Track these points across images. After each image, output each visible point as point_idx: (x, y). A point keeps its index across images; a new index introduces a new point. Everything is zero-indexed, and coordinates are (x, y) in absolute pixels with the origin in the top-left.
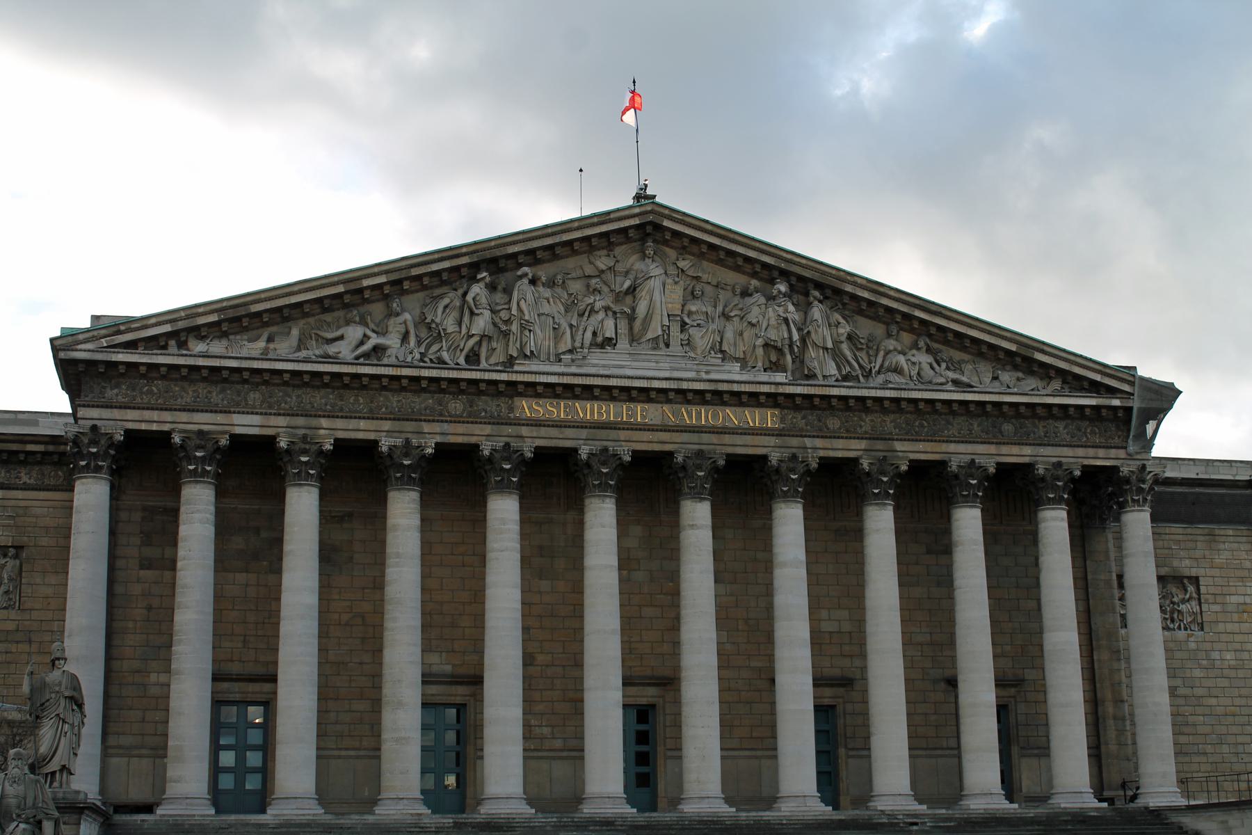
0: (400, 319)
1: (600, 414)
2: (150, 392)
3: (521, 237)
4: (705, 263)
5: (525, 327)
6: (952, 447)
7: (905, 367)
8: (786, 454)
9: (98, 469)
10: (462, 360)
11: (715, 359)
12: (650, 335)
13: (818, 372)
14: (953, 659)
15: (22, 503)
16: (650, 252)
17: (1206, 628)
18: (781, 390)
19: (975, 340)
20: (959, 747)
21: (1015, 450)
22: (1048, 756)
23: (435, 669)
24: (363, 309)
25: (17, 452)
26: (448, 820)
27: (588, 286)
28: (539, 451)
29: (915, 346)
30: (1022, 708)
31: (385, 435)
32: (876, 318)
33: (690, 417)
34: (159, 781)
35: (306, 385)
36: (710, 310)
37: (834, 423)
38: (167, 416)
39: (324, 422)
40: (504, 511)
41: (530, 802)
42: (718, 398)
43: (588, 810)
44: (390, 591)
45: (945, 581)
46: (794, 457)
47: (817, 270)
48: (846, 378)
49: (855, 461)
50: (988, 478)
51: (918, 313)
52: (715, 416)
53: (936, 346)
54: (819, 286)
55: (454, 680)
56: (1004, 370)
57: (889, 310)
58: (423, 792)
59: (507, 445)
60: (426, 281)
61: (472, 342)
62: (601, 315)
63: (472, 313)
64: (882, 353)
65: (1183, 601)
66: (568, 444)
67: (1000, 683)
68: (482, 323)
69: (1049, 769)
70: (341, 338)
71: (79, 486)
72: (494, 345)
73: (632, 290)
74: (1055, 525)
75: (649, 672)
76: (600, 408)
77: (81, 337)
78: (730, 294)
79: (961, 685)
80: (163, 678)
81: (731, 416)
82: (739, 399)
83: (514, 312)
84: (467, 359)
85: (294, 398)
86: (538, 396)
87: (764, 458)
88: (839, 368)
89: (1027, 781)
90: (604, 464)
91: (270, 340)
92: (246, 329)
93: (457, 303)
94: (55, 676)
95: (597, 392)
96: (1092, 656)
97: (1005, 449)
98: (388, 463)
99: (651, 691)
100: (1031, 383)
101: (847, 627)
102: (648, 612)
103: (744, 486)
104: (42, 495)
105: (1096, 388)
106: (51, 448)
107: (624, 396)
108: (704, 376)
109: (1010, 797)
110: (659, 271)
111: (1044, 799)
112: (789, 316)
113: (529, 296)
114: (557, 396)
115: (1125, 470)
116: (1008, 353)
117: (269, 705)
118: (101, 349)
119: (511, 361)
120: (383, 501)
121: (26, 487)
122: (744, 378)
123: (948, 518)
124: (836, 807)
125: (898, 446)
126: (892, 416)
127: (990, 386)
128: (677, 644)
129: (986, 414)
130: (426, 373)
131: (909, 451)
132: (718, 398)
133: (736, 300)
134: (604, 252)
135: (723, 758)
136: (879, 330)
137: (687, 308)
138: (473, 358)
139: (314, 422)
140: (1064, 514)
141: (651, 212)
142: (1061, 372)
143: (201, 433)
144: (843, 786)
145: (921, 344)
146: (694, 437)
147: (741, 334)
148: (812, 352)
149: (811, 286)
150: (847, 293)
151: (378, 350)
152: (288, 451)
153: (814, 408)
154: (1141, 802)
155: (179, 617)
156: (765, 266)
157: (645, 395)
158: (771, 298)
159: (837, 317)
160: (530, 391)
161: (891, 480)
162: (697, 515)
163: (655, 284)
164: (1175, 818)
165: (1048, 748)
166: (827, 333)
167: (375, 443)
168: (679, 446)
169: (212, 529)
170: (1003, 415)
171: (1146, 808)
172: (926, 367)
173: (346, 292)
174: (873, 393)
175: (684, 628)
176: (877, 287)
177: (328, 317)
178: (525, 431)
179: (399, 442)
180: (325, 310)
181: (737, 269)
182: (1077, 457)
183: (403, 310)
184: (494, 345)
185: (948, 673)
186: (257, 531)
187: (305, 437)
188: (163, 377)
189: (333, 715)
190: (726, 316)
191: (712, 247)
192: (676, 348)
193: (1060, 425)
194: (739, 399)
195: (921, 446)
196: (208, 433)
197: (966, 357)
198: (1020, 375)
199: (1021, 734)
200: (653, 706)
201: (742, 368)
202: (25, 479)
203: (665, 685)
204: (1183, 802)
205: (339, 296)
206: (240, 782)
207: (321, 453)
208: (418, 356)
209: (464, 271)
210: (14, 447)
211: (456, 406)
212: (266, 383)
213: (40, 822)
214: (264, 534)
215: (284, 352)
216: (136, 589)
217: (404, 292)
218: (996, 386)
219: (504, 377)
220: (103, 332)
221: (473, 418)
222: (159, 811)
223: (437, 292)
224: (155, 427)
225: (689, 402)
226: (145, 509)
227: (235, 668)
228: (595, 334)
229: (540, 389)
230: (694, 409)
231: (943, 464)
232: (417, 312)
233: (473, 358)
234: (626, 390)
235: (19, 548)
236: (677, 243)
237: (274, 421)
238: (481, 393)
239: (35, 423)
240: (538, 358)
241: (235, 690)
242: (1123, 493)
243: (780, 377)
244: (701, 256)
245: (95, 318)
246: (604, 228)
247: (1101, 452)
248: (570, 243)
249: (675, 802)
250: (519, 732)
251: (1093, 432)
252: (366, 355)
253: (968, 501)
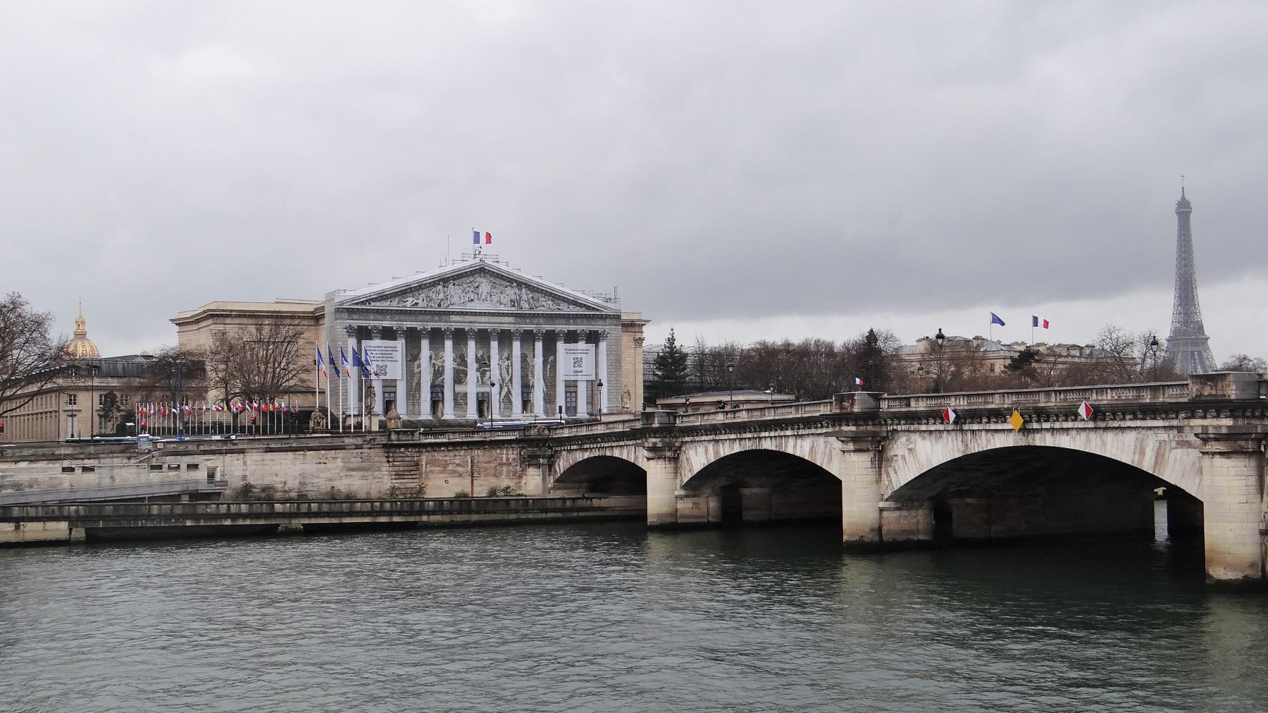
31: (418, 325)
42: (499, 315)
82: (503, 315)
103: (505, 338)
105: (594, 309)
127: (566, 309)
132: (499, 315)
157: (480, 314)
194: (503, 315)
221: (440, 321)
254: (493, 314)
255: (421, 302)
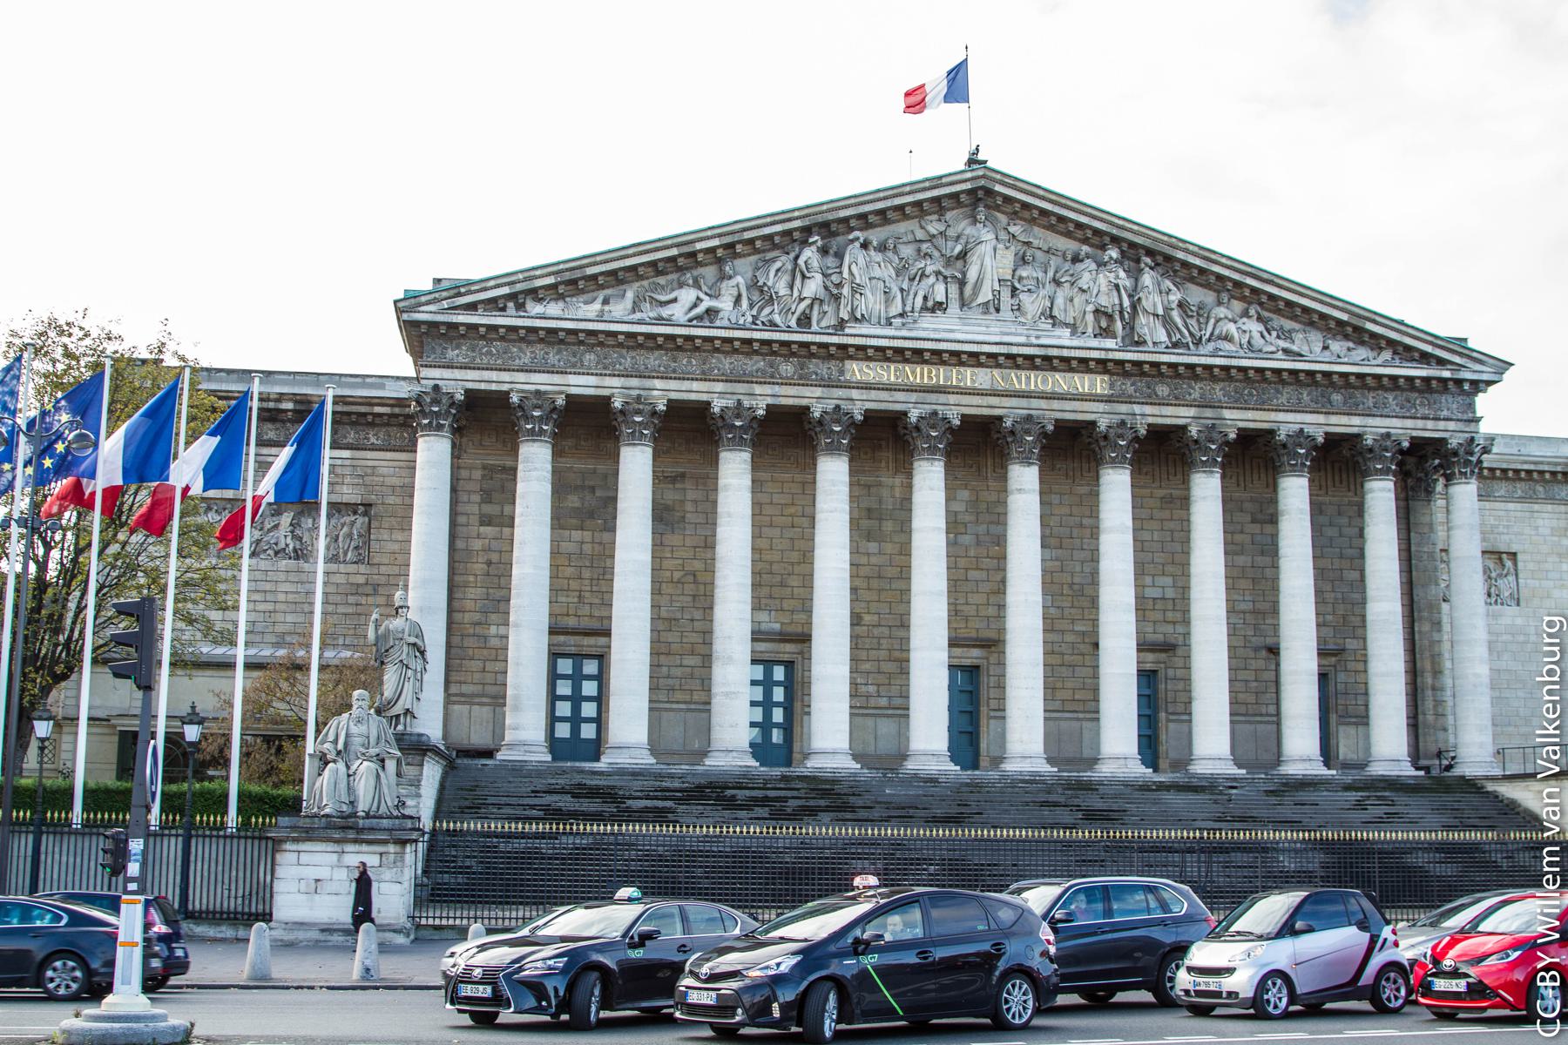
0: (733, 282)
1: (930, 378)
2: (489, 353)
3: (853, 201)
4: (1036, 229)
5: (856, 290)
6: (1281, 416)
7: (1236, 335)
8: (1116, 419)
9: (440, 427)
10: (793, 323)
11: (1045, 325)
12: (980, 300)
13: (1148, 338)
14: (1276, 627)
15: (370, 463)
16: (981, 217)
17: (1522, 603)
18: (1111, 355)
19: (1306, 310)
20: (1278, 714)
21: (1344, 420)
22: (1367, 724)
23: (764, 627)
24: (695, 273)
25: (365, 415)
26: (777, 772)
27: (919, 250)
28: (868, 414)
29: (1245, 314)
30: (1342, 677)
32: (1207, 286)
33: (1020, 382)
34: (498, 727)
35: (641, 346)
36: (1040, 275)
37: (1163, 390)
38: (505, 376)
39: (658, 383)
40: (833, 473)
41: (855, 757)
42: (1048, 363)
43: (911, 766)
44: (722, 549)
45: (1271, 550)
46: (1123, 423)
47: (1148, 237)
48: (1175, 345)
49: (1183, 429)
50: (1316, 448)
51: (1249, 281)
52: (1045, 381)
53: (1266, 314)
54: (1150, 253)
55: (784, 637)
56: (1334, 337)
57: (1219, 277)
58: (752, 745)
59: (838, 407)
60: (758, 244)
61: (803, 305)
62: (932, 279)
63: (804, 277)
64: (1212, 321)
65: (1500, 576)
66: (898, 407)
67: (1322, 653)
68: (813, 287)
69: (1367, 737)
70: (675, 300)
71: (422, 443)
72: (826, 308)
73: (963, 256)
74: (1381, 495)
75: (973, 634)
76: (930, 372)
77: (423, 299)
78: (1060, 260)
79: (1283, 653)
80: (502, 630)
81: (1060, 381)
82: (1067, 364)
83: (846, 275)
84: (799, 324)
85: (628, 360)
86: (869, 359)
87: (1093, 424)
88: (1169, 336)
89: (1346, 749)
90: (933, 427)
91: (606, 302)
92: (582, 292)
93: (789, 266)
94: (396, 624)
95: (927, 356)
96: (1412, 628)
97: (1334, 419)
98: (720, 424)
99: (976, 652)
100: (1362, 353)
101: (1170, 593)
102: (973, 574)
103: (1071, 449)
104: (389, 455)
105: (1425, 358)
106: (397, 410)
107: (954, 360)
108: (1035, 341)
109: (1327, 764)
110: (991, 236)
111: (1363, 766)
112: (1121, 283)
113: (861, 261)
114: (888, 360)
115: (1454, 442)
116: (1340, 323)
117: (602, 658)
118: (442, 311)
119: (841, 324)
120: (714, 462)
121: (374, 448)
122: (1075, 343)
123: (1275, 488)
124: (1156, 770)
125: (1227, 414)
126: (1222, 384)
128: (1002, 607)
129: (1316, 384)
130: (757, 335)
131: (1237, 419)
132: (1048, 363)
133: (1067, 265)
134: (935, 217)
135: (1046, 719)
136: (1209, 297)
137: (1018, 273)
138: (804, 321)
139: (648, 383)
140: (1391, 485)
141: (983, 177)
142: (1391, 343)
143: (538, 392)
144: (1162, 749)
145: (1252, 312)
146: (1023, 402)
147: (1071, 300)
148: (1142, 319)
149: (1142, 252)
150: (1179, 260)
151: (711, 313)
152: (621, 412)
153: (1143, 374)
154: (1457, 772)
155: (516, 571)
156: (1097, 232)
157: (975, 359)
158: (1101, 264)
159: (1168, 283)
160: (861, 354)
161: (1220, 448)
162: (1025, 479)
163: (986, 249)
164: (1490, 787)
165: (1367, 717)
166: (1158, 299)
167: (708, 403)
168: (1010, 410)
169: (549, 487)
170: (1332, 385)
171: (1463, 777)
172: (1256, 336)
173: (680, 255)
174: (1203, 360)
175: (1010, 590)
176: (1208, 254)
177: (662, 280)
178: (855, 394)
179: (730, 403)
180: (659, 273)
181: (1068, 235)
182: (1404, 428)
183: (736, 274)
184: (826, 308)
185: (1270, 641)
186: (593, 489)
187: (639, 397)
188: (502, 339)
189: (665, 669)
190: (1057, 282)
191: (1044, 212)
192: (1006, 313)
193: (1390, 397)
194: (1067, 364)
195: (1250, 415)
196: (545, 393)
197: (1297, 326)
198: (1351, 345)
199: (1341, 701)
200: (977, 667)
201: (1073, 334)
202: (373, 440)
203: (989, 646)
204: (1498, 772)
205: (672, 259)
206: (575, 730)
207: (654, 413)
208: (750, 319)
209: (796, 235)
210: (363, 409)
211: (787, 368)
212: (601, 344)
213: (383, 761)
214: (598, 493)
215: (618, 312)
216: (477, 545)
217: (736, 256)
218: (1326, 356)
219: (835, 340)
220: (445, 294)
221: (803, 380)
222: (500, 756)
223: (769, 255)
224: (494, 387)
225: (1018, 367)
226: (484, 467)
227: (571, 622)
228: (925, 298)
229: (870, 352)
230: (1023, 374)
231: (1272, 432)
232: (749, 275)
233: (804, 321)
234: (955, 354)
235: (368, 506)
236: (1009, 209)
237: (609, 381)
238: (812, 355)
239: (382, 386)
240: (869, 322)
241: (570, 643)
242: (1450, 465)
243: (1110, 343)
244: (1032, 221)
245: (438, 281)
246: (935, 193)
247: (1430, 424)
248: (901, 208)
249: (998, 760)
250: (845, 689)
251: (1422, 404)
252: (699, 318)
253: (1295, 470)
254: (1030, 362)
255: (731, 308)
